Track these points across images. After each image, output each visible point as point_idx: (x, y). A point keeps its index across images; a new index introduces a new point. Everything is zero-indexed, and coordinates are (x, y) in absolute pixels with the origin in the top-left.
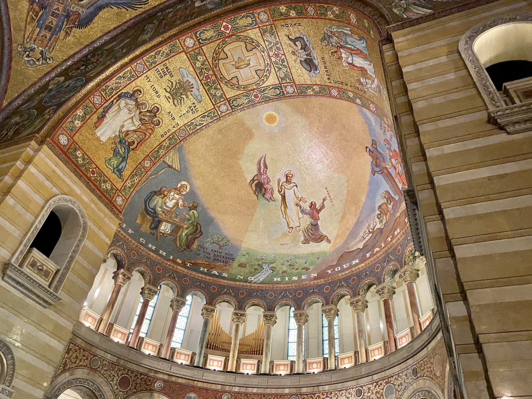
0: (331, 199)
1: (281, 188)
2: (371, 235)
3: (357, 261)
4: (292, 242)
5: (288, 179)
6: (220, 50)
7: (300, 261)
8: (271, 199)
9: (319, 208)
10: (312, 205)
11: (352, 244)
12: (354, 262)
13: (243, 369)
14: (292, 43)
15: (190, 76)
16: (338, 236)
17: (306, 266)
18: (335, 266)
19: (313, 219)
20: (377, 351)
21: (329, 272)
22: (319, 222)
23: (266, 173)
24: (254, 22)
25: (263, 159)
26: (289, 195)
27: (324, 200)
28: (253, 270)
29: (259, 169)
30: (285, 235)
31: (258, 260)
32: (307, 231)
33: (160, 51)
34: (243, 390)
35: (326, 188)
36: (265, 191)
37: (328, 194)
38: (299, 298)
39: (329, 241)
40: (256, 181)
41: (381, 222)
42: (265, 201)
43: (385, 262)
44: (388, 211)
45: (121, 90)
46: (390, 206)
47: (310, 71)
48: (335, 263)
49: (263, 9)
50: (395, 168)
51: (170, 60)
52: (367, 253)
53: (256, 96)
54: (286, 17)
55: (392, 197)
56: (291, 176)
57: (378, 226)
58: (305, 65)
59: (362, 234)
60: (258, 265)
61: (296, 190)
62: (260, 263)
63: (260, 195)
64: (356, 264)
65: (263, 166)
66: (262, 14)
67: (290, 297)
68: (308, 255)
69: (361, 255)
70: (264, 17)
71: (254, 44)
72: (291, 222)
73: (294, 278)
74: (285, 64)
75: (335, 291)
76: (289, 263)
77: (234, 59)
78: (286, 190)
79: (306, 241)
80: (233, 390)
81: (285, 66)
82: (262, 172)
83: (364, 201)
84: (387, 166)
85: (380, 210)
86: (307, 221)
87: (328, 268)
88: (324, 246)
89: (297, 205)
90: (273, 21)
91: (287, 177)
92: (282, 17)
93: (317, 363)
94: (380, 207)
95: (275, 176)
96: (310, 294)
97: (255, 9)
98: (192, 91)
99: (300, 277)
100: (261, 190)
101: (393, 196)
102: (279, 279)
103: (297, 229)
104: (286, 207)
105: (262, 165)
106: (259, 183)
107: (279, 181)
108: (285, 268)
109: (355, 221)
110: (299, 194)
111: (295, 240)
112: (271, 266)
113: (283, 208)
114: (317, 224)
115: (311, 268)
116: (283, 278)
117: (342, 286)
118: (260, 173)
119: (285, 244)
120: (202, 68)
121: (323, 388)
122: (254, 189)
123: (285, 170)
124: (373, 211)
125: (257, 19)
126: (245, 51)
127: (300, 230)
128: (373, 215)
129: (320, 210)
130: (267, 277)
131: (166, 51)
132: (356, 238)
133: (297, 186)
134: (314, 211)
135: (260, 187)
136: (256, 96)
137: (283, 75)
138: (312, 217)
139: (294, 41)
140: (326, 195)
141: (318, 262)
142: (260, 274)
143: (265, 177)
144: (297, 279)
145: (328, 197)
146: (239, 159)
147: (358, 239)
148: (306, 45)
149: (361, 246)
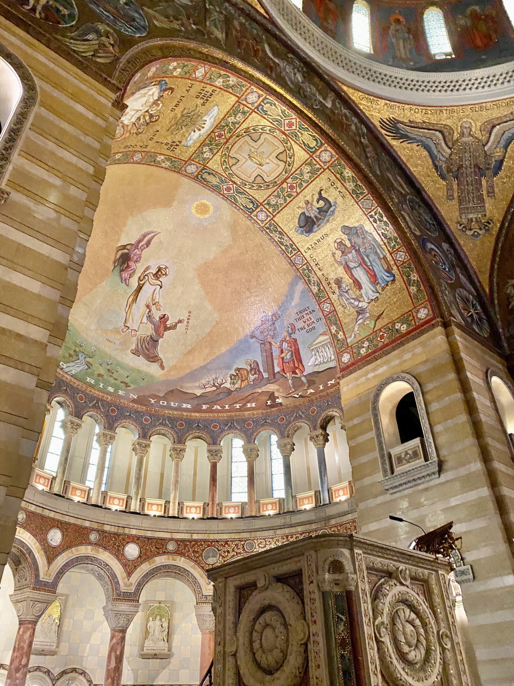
0: (187, 326)
1: (144, 277)
2: (215, 388)
3: (189, 406)
4: (121, 344)
5: (159, 273)
6: (260, 130)
7: (121, 371)
8: (126, 281)
9: (168, 326)
10: (164, 318)
11: (189, 385)
12: (184, 406)
13: (109, 503)
14: (316, 196)
15: (212, 120)
16: (174, 367)
17: (127, 380)
18: (159, 398)
19: (156, 333)
20: (194, 509)
21: (153, 401)
22: (161, 341)
23: (142, 250)
24: (314, 149)
25: (153, 234)
26: (148, 289)
27: (180, 321)
28: (67, 355)
29: (139, 241)
30: (116, 331)
31: (76, 345)
32: (142, 341)
33: (229, 77)
34: (39, 511)
35: (190, 312)
36: (126, 268)
37: (188, 319)
38: (113, 416)
39: (162, 367)
40: (126, 251)
41: (234, 384)
42: (118, 279)
43: (226, 425)
44: (247, 379)
45: (166, 77)
46: (252, 377)
47: (300, 227)
48: (162, 395)
49: (334, 153)
50: (282, 352)
51: (222, 92)
52: (204, 404)
53: (228, 189)
54: (342, 179)
55: (259, 371)
56: (164, 273)
57: (228, 385)
58: (303, 217)
59: (204, 381)
60: (75, 351)
61: (157, 291)
62: (77, 350)
63: (118, 268)
64: (187, 410)
65: (145, 241)
66: (328, 153)
67: (102, 410)
68: (133, 370)
69: (196, 402)
70: (326, 156)
71: (288, 159)
72: (131, 321)
73: (110, 388)
74: (288, 200)
75: (155, 426)
76: (108, 367)
77: (258, 148)
78: (148, 282)
79: (136, 352)
80: (29, 508)
81: (285, 200)
82: (140, 245)
83: (223, 352)
84: (273, 343)
85: (237, 372)
86: (148, 330)
87: (154, 397)
88: (153, 369)
89: (148, 306)
90: (328, 168)
91: (159, 271)
92: (338, 176)
93: (119, 499)
94: (238, 369)
95: (148, 260)
96: (125, 417)
97: (329, 145)
98: (194, 132)
99: (116, 390)
100: (123, 263)
101: (262, 370)
102: (93, 382)
103: (133, 333)
104: (135, 300)
105: (146, 239)
106: (127, 254)
107: (148, 268)
108: (102, 371)
109: (202, 364)
110: (157, 296)
111: (125, 343)
112: (88, 359)
113: (131, 299)
114: (157, 341)
115: (133, 386)
116: (97, 382)
117: (165, 425)
118: (136, 246)
119: (111, 342)
120: (227, 125)
121: (130, 531)
122: (118, 257)
123: (162, 263)
124: (229, 368)
125: (319, 151)
126: (275, 154)
127: (135, 335)
128: (226, 371)
129: (169, 329)
130: (80, 371)
131: (231, 82)
132: (196, 381)
133: (161, 287)
134: (162, 325)
135: (124, 260)
136: (228, 189)
137: (274, 203)
138: (157, 330)
139: (321, 198)
140: (184, 317)
141: (143, 384)
142: (73, 364)
143: (138, 253)
144: (112, 391)
145: (185, 322)
146: (132, 215)
147: (197, 384)
148: (327, 212)
149: (198, 392)
